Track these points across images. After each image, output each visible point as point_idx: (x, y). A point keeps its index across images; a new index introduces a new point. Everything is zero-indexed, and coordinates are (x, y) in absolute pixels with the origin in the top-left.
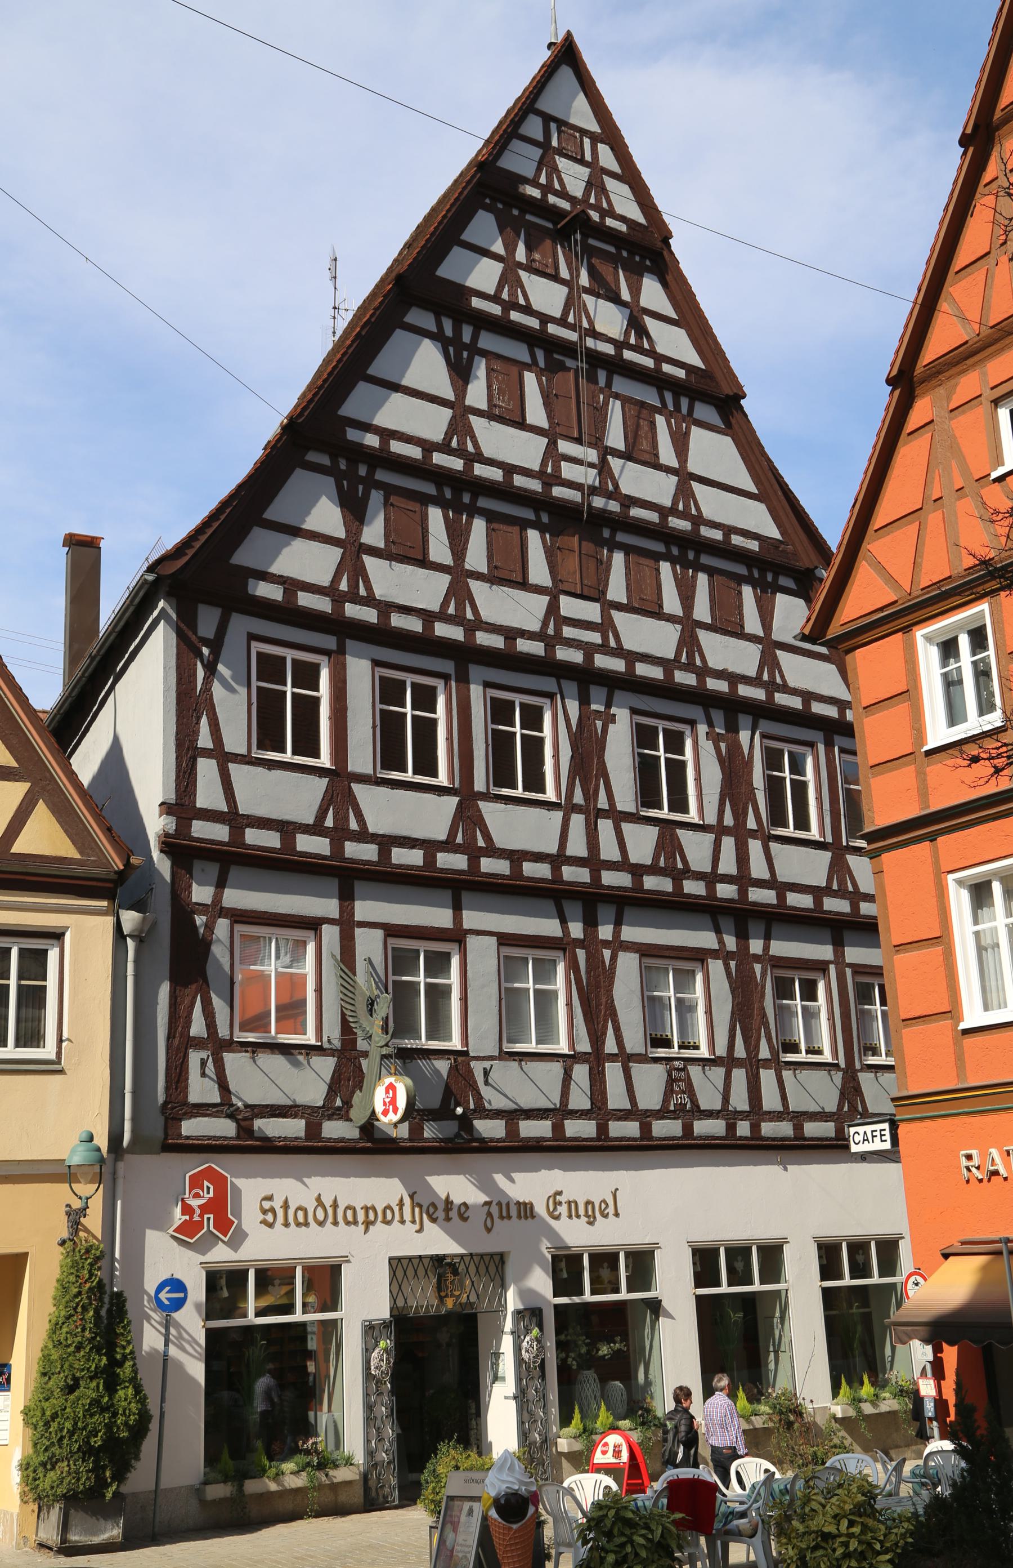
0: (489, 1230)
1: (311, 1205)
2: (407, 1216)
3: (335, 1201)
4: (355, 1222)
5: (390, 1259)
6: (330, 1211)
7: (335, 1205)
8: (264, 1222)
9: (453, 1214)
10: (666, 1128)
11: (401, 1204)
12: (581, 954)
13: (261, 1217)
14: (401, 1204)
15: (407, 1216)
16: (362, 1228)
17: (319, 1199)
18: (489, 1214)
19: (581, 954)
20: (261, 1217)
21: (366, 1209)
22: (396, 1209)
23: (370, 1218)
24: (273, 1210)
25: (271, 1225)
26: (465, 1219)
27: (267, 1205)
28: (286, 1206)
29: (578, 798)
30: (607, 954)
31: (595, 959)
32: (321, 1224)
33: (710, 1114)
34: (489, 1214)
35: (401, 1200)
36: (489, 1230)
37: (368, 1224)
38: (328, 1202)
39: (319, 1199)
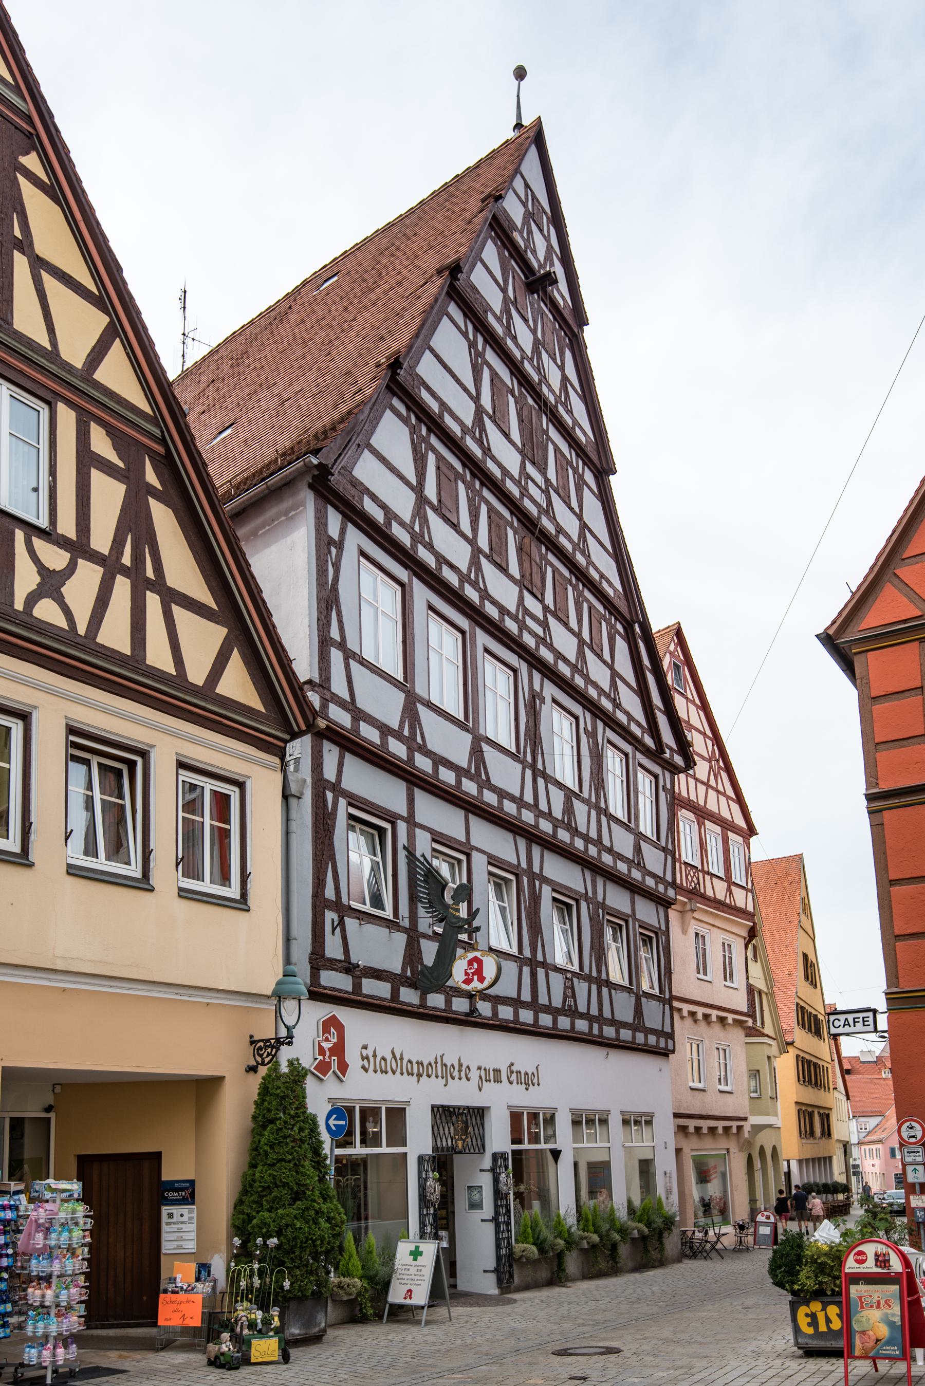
0: (480, 1090)
1: (389, 1057)
2: (440, 1074)
3: (402, 1055)
4: (412, 1075)
5: (433, 1107)
6: (399, 1061)
7: (402, 1059)
8: (363, 1067)
9: (463, 1074)
10: (564, 1022)
11: (436, 1063)
12: (525, 879)
13: (361, 1063)
14: (436, 1063)
15: (440, 1074)
16: (415, 1078)
17: (393, 1053)
18: (480, 1077)
19: (525, 879)
20: (361, 1063)
21: (417, 1063)
22: (434, 1065)
23: (420, 1070)
24: (367, 1058)
25: (366, 1070)
26: (468, 1079)
27: (365, 1052)
28: (375, 1056)
29: (529, 758)
30: (537, 883)
31: (532, 885)
32: (394, 1073)
33: (582, 1016)
34: (480, 1077)
35: (436, 1059)
36: (480, 1090)
37: (420, 1075)
38: (398, 1057)
39: (393, 1053)
